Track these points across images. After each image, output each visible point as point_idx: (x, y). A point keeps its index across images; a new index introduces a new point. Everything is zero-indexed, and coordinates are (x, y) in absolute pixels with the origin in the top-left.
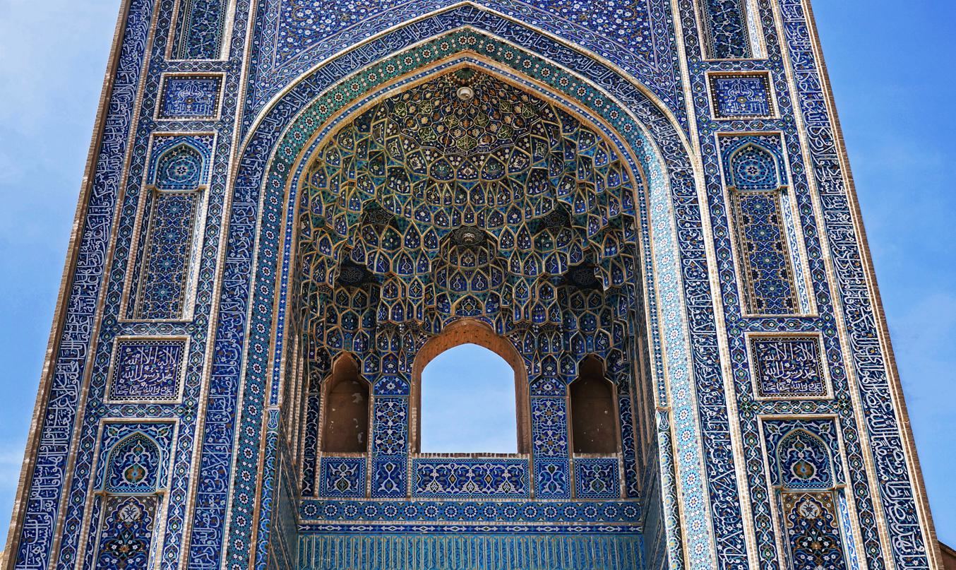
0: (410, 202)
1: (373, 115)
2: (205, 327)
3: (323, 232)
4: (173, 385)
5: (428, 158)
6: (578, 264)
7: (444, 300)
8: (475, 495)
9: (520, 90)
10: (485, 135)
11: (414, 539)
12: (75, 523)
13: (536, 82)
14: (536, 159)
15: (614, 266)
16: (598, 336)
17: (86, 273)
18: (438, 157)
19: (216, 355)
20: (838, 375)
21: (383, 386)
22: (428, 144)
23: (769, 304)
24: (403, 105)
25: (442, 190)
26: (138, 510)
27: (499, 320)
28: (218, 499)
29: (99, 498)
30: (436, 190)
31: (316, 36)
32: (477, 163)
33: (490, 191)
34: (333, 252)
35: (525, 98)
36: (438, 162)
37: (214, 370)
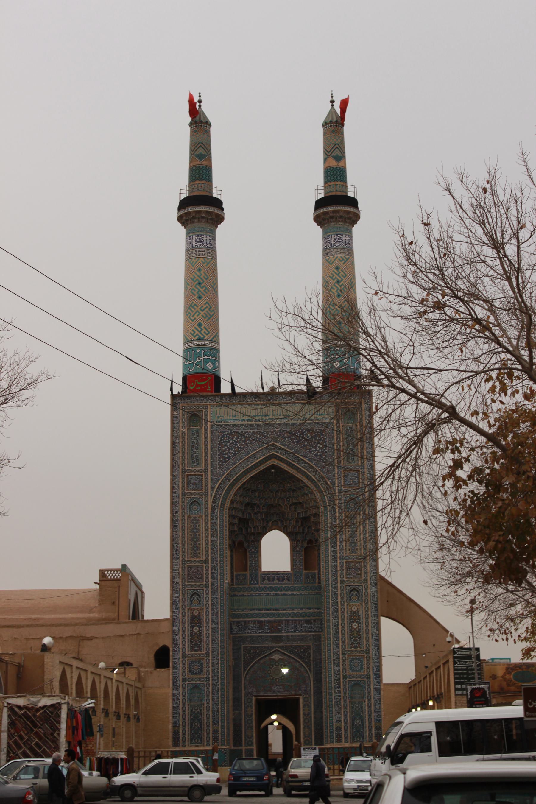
2: (208, 561)
4: (202, 578)
8: (277, 584)
11: (261, 597)
12: (184, 616)
13: (293, 470)
14: (294, 486)
17: (175, 545)
19: (212, 569)
20: (366, 573)
21: (251, 550)
23: (352, 550)
26: (198, 612)
28: (217, 608)
29: (188, 609)
31: (229, 458)
34: (236, 521)
37: (212, 573)
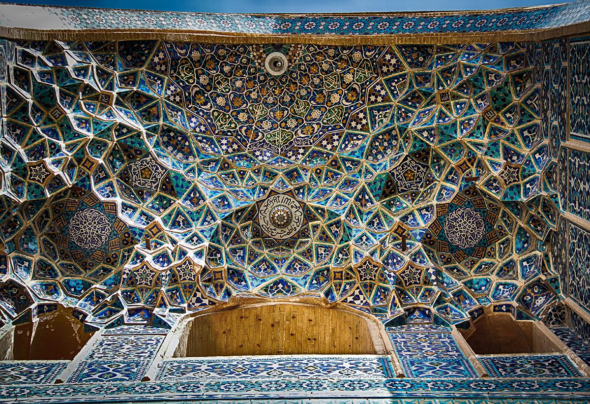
0: (192, 170)
1: (147, 58)
3: (51, 120)
5: (224, 147)
6: (449, 201)
7: (240, 281)
9: (349, 48)
10: (304, 126)
15: (507, 151)
16: (497, 288)
18: (238, 150)
22: (224, 133)
24: (191, 70)
25: (242, 178)
27: (328, 293)
30: (234, 177)
32: (293, 158)
33: (312, 179)
35: (357, 56)
36: (239, 156)
